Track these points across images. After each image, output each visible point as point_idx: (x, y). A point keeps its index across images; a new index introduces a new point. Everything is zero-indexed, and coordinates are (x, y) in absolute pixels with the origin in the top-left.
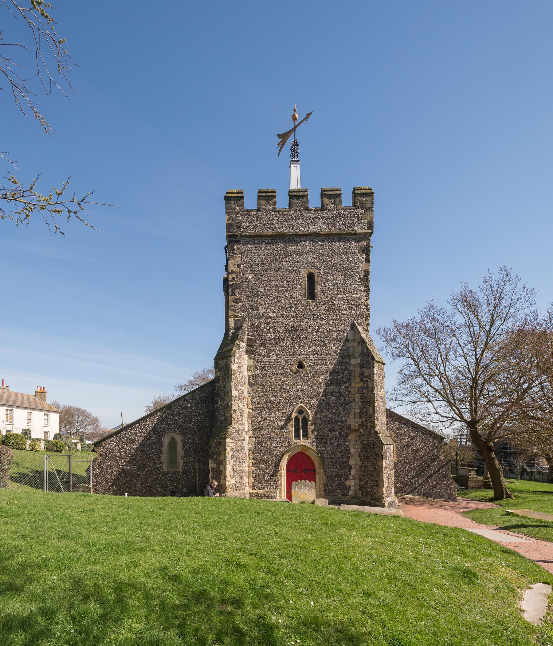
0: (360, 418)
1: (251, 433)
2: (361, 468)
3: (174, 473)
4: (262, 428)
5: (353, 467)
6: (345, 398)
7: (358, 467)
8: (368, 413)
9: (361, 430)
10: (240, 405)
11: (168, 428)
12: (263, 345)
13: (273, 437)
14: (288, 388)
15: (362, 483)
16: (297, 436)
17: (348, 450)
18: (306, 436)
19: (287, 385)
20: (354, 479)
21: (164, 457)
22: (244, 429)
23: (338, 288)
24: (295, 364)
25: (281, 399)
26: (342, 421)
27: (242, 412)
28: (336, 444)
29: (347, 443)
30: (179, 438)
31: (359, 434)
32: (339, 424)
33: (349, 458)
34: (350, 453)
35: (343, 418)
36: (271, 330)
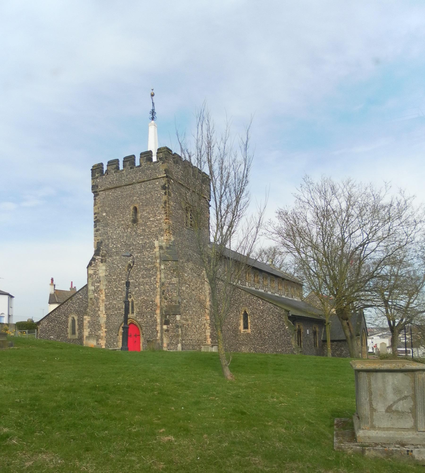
1: (104, 312)
3: (74, 340)
4: (109, 309)
5: (159, 332)
6: (154, 286)
10: (96, 295)
12: (111, 256)
13: (115, 314)
14: (123, 282)
17: (156, 320)
18: (133, 313)
19: (122, 280)
21: (69, 330)
22: (99, 310)
23: (149, 214)
24: (127, 265)
25: (119, 289)
26: (152, 301)
27: (97, 299)
28: (149, 317)
29: (155, 316)
32: (151, 303)
33: (156, 326)
34: (157, 322)
35: (153, 299)
36: (115, 246)
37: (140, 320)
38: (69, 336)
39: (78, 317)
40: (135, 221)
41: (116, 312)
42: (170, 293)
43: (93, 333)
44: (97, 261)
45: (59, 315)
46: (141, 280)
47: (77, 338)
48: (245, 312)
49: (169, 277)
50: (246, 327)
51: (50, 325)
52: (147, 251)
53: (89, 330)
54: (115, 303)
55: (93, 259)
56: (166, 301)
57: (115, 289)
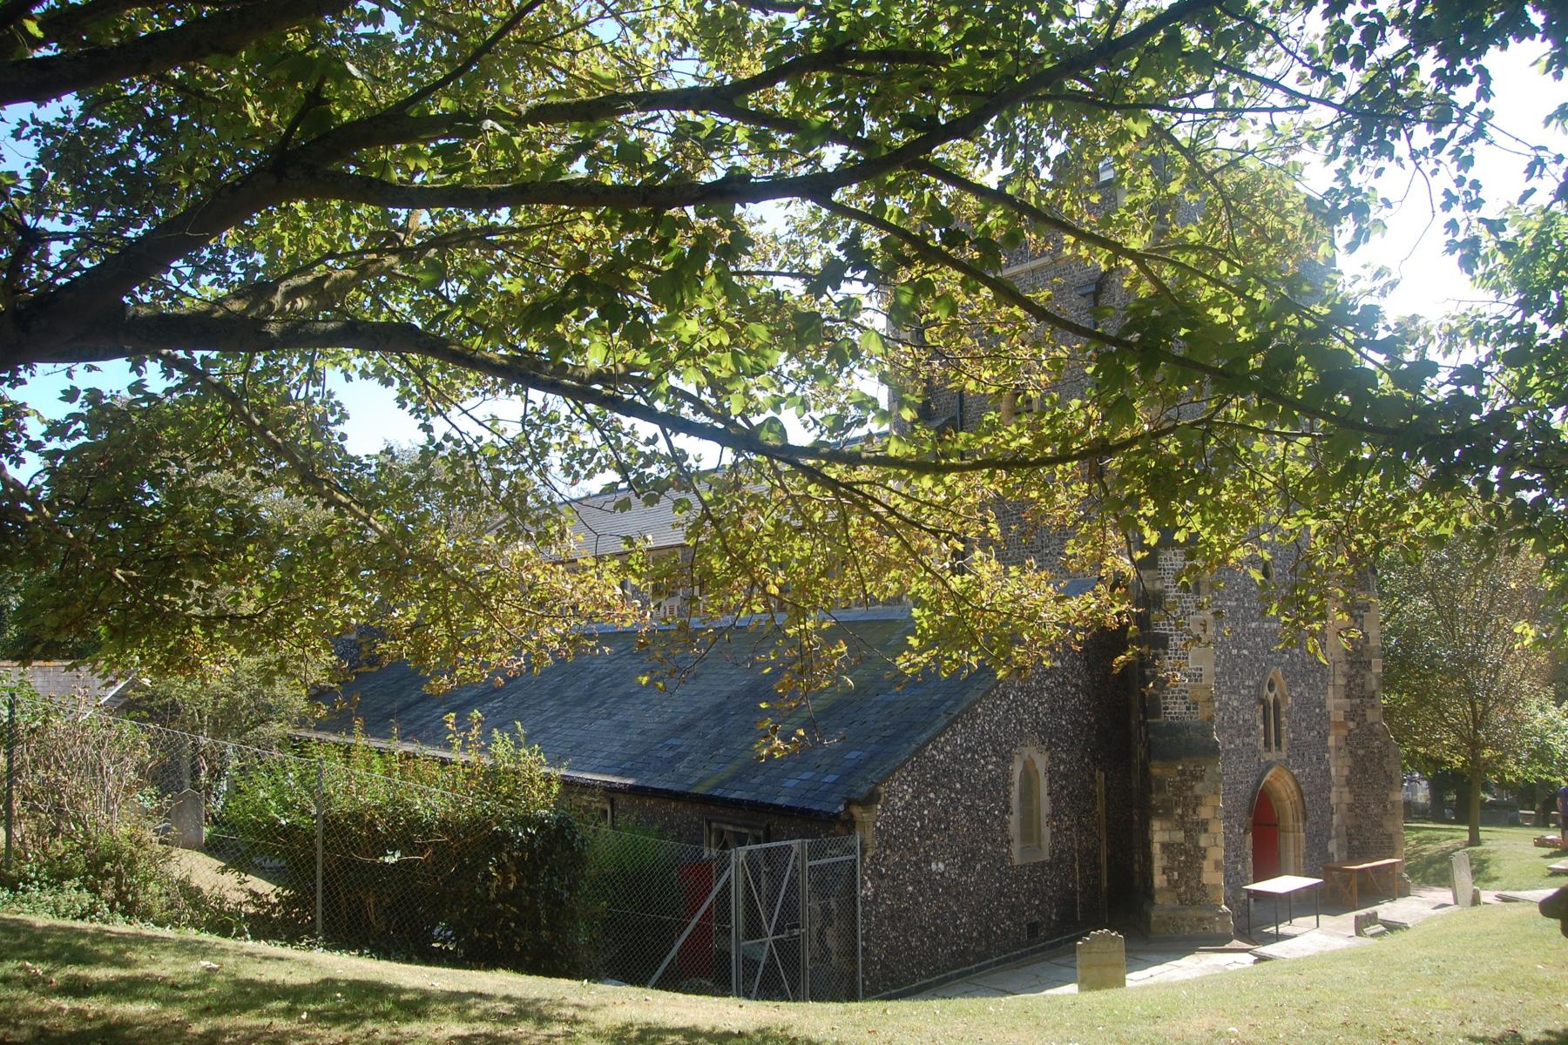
0: (1348, 697)
2: (1350, 810)
7: (1344, 807)
8: (1367, 687)
9: (1352, 725)
11: (1021, 734)
14: (1254, 625)
15: (1356, 843)
16: (1267, 744)
18: (1278, 743)
20: (1337, 836)
30: (1042, 763)
31: (1345, 733)
38: (1016, 854)
39: (1051, 758)
45: (968, 749)
47: (1047, 857)
51: (930, 803)
54: (1235, 704)
57: (1235, 652)
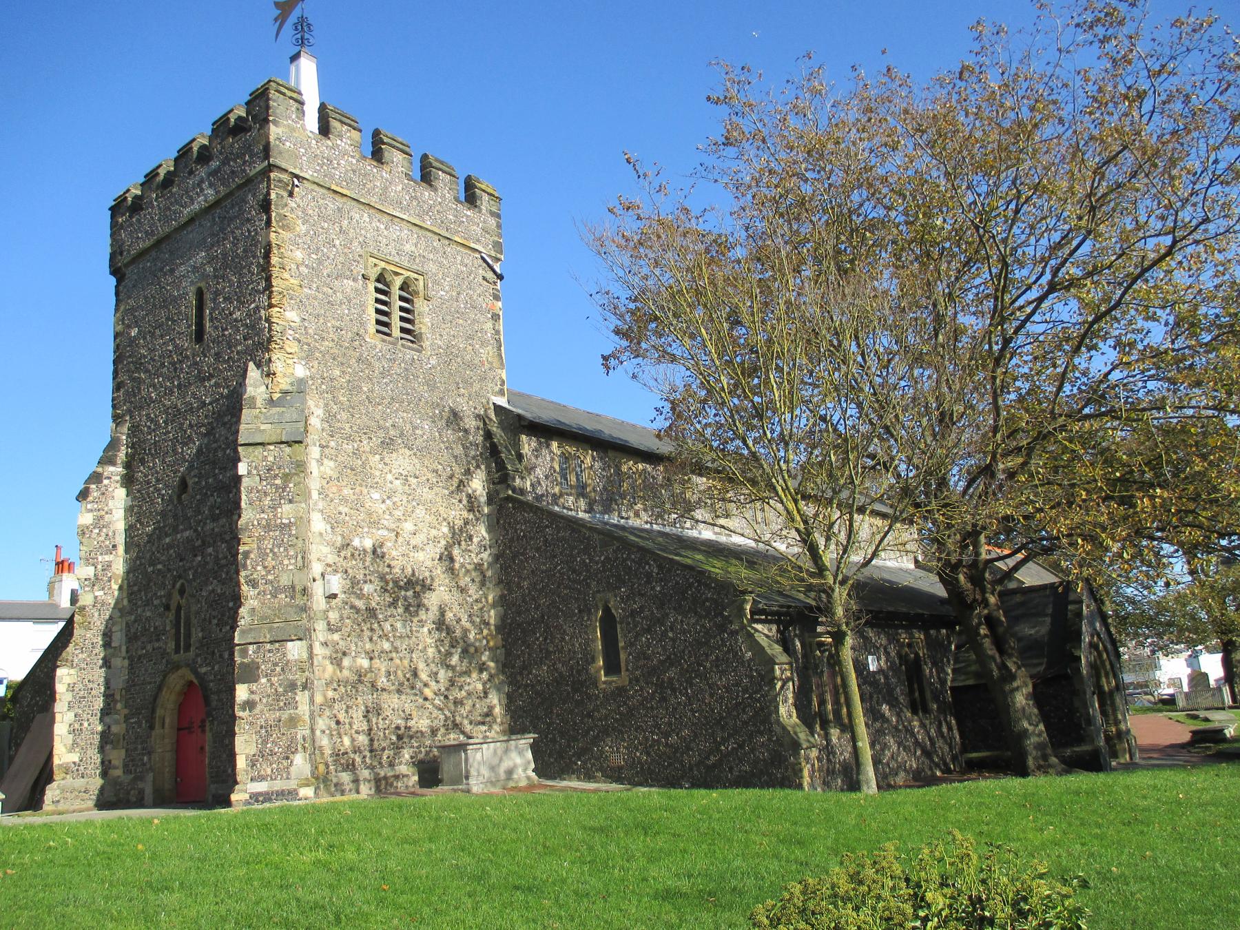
10: (99, 593)
37: (203, 670)
40: (199, 335)
41: (149, 647)
42: (270, 562)
43: (86, 724)
44: (106, 482)
46: (210, 526)
48: (607, 610)
49: (267, 501)
50: (612, 667)
52: (224, 424)
53: (70, 716)
54: (148, 614)
55: (96, 478)
56: (253, 592)
57: (150, 569)
